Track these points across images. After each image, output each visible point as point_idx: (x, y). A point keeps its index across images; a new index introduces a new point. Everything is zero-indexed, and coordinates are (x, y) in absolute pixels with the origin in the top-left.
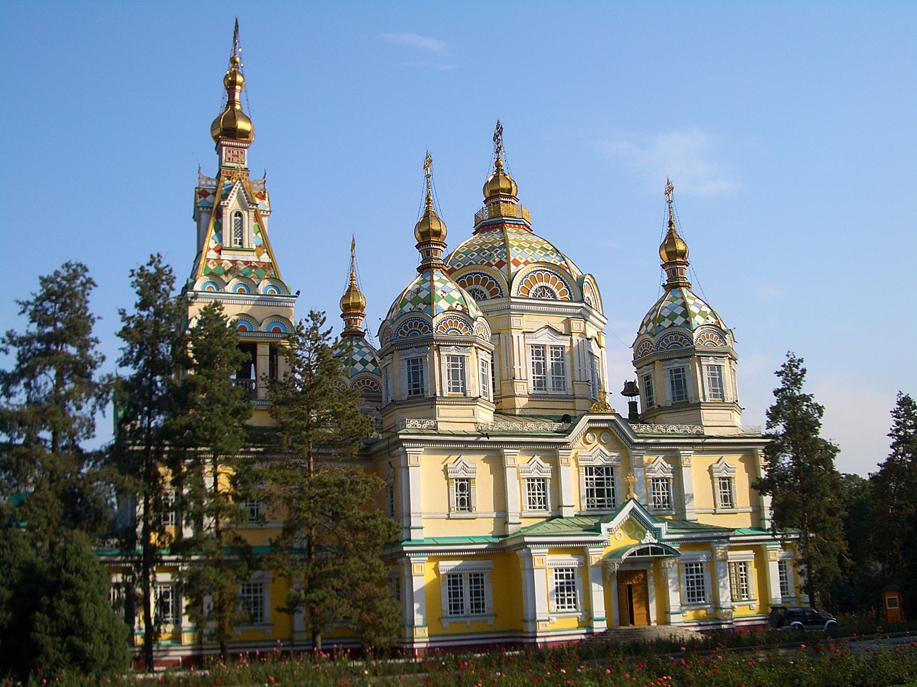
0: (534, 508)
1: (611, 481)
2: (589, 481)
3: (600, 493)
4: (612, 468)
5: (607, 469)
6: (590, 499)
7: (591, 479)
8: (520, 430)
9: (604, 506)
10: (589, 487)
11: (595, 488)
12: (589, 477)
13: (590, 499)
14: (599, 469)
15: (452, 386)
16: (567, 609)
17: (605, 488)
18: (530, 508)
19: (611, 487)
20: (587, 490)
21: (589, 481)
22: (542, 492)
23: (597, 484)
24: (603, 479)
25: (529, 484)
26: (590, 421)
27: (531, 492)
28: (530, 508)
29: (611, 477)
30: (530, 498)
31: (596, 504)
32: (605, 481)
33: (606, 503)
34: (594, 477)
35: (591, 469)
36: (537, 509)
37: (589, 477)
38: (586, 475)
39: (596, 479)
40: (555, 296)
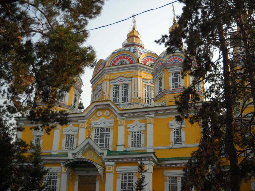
1: (108, 135)
5: (107, 129)
7: (98, 134)
9: (103, 147)
10: (96, 138)
14: (102, 129)
17: (105, 138)
19: (108, 138)
21: (96, 135)
23: (101, 137)
25: (67, 138)
26: (96, 106)
28: (66, 148)
30: (66, 144)
32: (105, 135)
33: (104, 146)
35: (98, 130)
37: (96, 133)
38: (96, 132)
39: (100, 134)
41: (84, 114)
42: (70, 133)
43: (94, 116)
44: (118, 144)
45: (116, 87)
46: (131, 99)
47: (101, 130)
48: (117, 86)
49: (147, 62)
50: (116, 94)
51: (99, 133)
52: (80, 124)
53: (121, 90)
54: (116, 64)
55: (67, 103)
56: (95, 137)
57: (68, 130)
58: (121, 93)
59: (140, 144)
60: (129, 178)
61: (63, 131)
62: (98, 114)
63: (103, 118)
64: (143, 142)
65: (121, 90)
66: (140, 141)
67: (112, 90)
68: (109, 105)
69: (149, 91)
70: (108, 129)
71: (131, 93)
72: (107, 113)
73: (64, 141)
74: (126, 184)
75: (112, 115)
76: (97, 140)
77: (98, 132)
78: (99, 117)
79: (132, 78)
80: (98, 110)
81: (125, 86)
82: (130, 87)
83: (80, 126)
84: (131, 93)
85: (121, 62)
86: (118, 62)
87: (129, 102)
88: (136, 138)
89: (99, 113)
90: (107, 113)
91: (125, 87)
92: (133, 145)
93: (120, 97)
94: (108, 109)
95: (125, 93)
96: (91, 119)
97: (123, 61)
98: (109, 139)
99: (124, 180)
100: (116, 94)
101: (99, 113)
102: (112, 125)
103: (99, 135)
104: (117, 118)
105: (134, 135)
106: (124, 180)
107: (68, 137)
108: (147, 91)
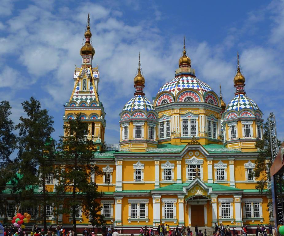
0: (167, 180)
2: (190, 170)
3: (194, 174)
4: (200, 165)
6: (190, 176)
7: (191, 169)
8: (162, 151)
10: (190, 172)
11: (192, 172)
12: (190, 168)
13: (190, 176)
14: (194, 165)
15: (137, 136)
16: (169, 219)
18: (165, 180)
20: (189, 173)
21: (190, 170)
22: (170, 174)
23: (193, 171)
27: (166, 174)
28: (165, 180)
31: (192, 178)
34: (192, 168)
36: (168, 180)
37: (190, 168)
39: (193, 169)
40: (193, 101)
41: (180, 155)
43: (187, 155)
44: (208, 179)
45: (185, 121)
47: (193, 166)
50: (185, 127)
51: (192, 168)
53: (189, 124)
56: (189, 171)
58: (189, 127)
59: (224, 178)
60: (227, 206)
62: (189, 154)
64: (226, 177)
65: (189, 124)
66: (224, 176)
67: (182, 123)
70: (198, 166)
71: (199, 128)
74: (225, 210)
75: (201, 155)
76: (191, 174)
77: (191, 167)
78: (192, 156)
79: (199, 115)
80: (190, 151)
81: (193, 121)
82: (197, 123)
85: (188, 98)
88: (221, 174)
89: (191, 154)
90: (197, 154)
92: (219, 179)
93: (189, 130)
94: (198, 151)
95: (193, 127)
96: (185, 157)
97: (190, 98)
98: (200, 173)
99: (223, 207)
100: (185, 127)
103: (192, 170)
105: (219, 172)
106: (223, 207)
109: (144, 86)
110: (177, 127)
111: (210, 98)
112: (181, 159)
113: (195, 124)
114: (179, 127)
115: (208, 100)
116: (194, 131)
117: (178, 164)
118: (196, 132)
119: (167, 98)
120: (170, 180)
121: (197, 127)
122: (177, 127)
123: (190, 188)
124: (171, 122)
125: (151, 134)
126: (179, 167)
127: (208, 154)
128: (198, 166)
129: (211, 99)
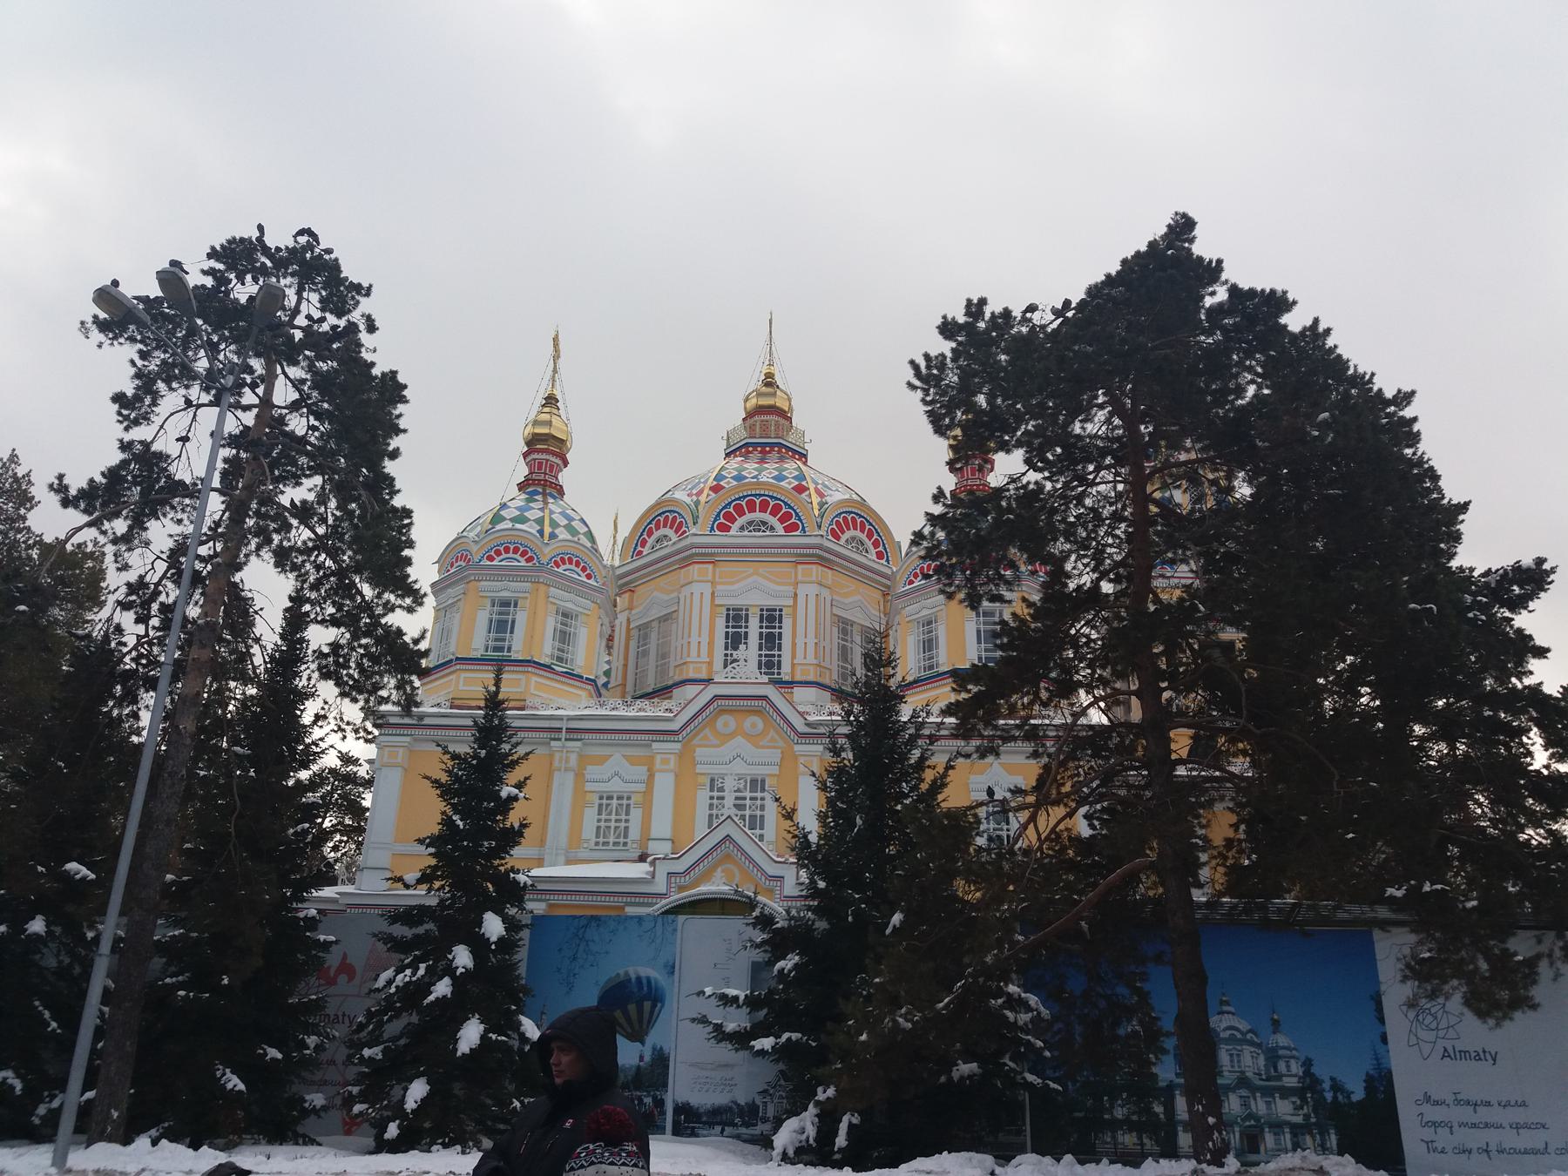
1: (759, 802)
4: (763, 781)
19: (758, 813)
21: (715, 801)
22: (623, 817)
24: (745, 799)
26: (716, 697)
29: (759, 795)
30: (598, 828)
41: (675, 726)
42: (616, 786)
43: (707, 731)
45: (736, 617)
46: (793, 665)
48: (742, 610)
49: (843, 532)
52: (658, 758)
53: (754, 628)
54: (735, 527)
55: (580, 667)
57: (605, 777)
61: (588, 777)
63: (739, 739)
65: (754, 628)
67: (721, 623)
68: (764, 698)
69: (847, 641)
71: (794, 645)
72: (754, 723)
73: (590, 818)
75: (772, 733)
78: (732, 735)
80: (723, 711)
81: (771, 617)
82: (787, 622)
83: (658, 765)
84: (794, 645)
86: (741, 521)
87: (786, 674)
89: (726, 725)
90: (754, 725)
91: (771, 619)
95: (771, 641)
96: (694, 742)
98: (762, 817)
101: (726, 725)
102: (775, 770)
104: (797, 748)
107: (604, 801)
108: (843, 640)
109: (566, 463)
110: (700, 636)
111: (855, 529)
112: (678, 746)
113: (780, 628)
114: (705, 640)
115: (844, 537)
116: (774, 656)
117: (661, 771)
118: (779, 662)
119: (671, 528)
120: (621, 847)
121: (786, 642)
122: (700, 636)
123: (687, 872)
124: (677, 618)
125: (563, 641)
126: (664, 785)
127: (802, 728)
128: (754, 782)
129: (858, 533)
